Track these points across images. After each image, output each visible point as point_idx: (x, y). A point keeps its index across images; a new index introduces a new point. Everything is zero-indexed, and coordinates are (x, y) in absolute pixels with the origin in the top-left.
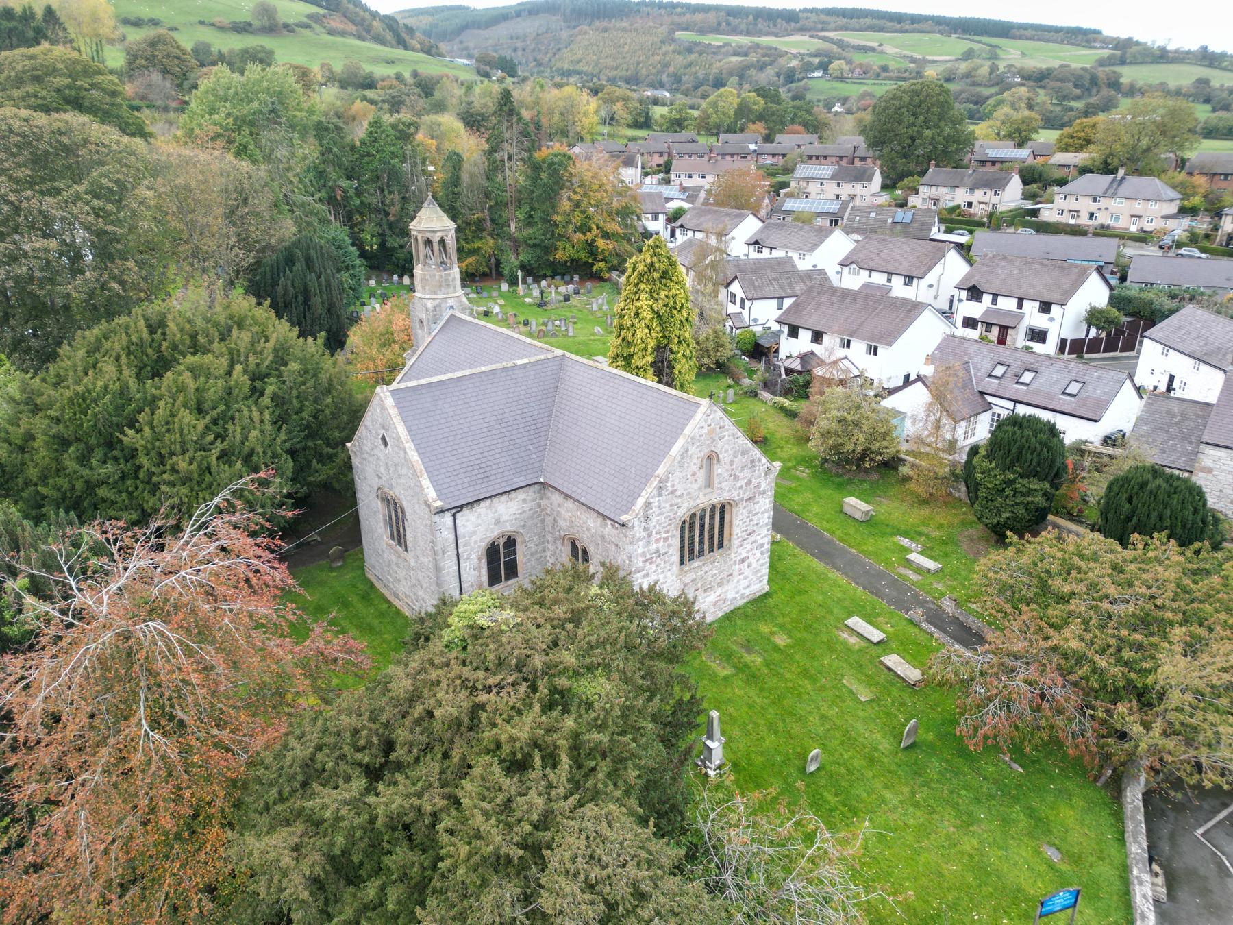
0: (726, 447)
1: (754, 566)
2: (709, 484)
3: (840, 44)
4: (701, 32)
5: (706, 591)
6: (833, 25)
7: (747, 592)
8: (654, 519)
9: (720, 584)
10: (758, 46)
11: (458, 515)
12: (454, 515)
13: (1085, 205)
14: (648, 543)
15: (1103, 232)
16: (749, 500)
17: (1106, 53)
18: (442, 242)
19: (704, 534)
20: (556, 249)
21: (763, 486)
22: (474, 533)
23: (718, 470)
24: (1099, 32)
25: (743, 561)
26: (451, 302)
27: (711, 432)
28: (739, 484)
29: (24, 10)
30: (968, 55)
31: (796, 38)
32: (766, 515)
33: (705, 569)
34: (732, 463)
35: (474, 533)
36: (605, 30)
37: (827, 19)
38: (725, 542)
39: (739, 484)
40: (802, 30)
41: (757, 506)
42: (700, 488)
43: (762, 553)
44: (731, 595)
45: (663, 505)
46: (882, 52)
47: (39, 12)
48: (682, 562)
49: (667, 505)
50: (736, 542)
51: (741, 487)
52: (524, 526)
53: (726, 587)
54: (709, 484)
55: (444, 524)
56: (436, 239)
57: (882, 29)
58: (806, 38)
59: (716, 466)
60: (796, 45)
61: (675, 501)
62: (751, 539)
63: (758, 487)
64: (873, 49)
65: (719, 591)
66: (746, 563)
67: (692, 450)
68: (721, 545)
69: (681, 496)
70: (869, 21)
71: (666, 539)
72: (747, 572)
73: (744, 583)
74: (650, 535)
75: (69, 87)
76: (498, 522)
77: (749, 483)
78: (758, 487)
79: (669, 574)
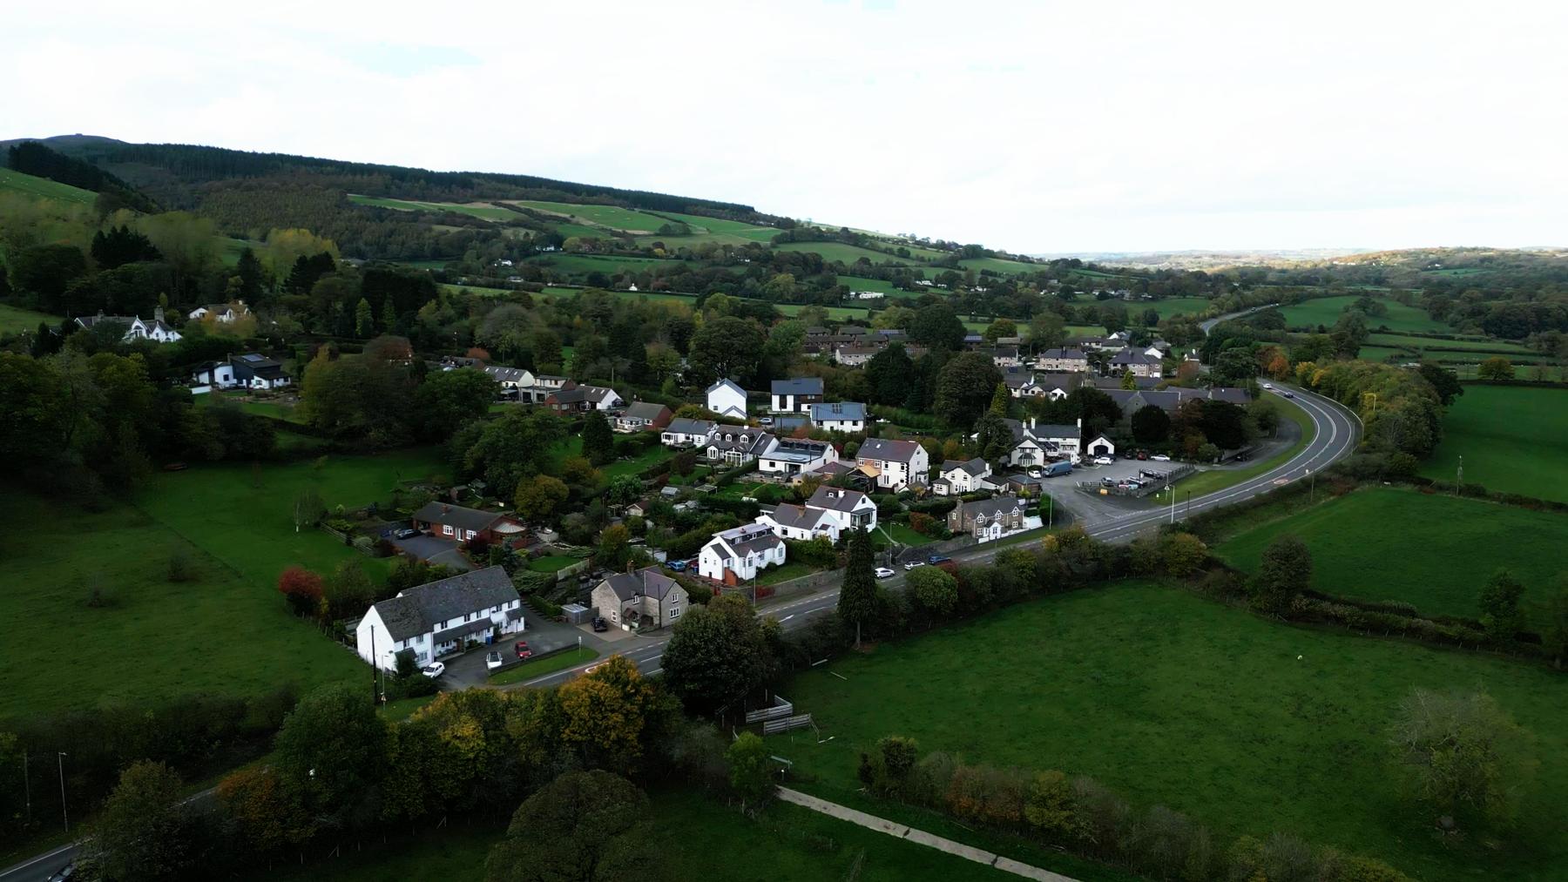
3: (528, 212)
4: (373, 195)
6: (512, 194)
10: (453, 214)
13: (1053, 362)
15: (1064, 372)
17: (779, 232)
24: (752, 209)
30: (666, 232)
31: (479, 205)
36: (249, 188)
37: (507, 187)
40: (482, 197)
46: (577, 224)
57: (563, 200)
58: (489, 206)
60: (482, 209)
64: (566, 220)
70: (549, 192)
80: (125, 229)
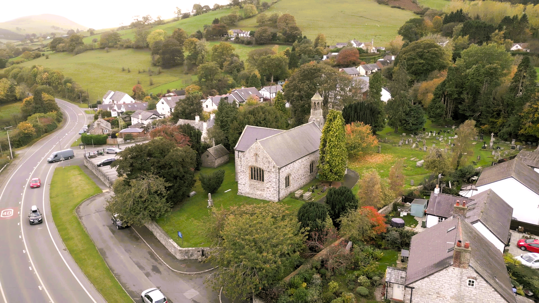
2: (256, 161)
7: (270, 198)
8: (242, 163)
9: (261, 190)
18: (315, 103)
19: (257, 174)
20: (521, 129)
21: (273, 170)
23: (259, 159)
25: (268, 188)
26: (314, 119)
27: (256, 148)
29: (514, 17)
33: (256, 183)
44: (265, 196)
47: (520, 17)
48: (252, 178)
54: (256, 161)
56: (313, 102)
62: (270, 183)
65: (261, 192)
67: (251, 150)
68: (263, 181)
73: (268, 195)
75: (421, 52)
77: (268, 167)
80: (461, 10)
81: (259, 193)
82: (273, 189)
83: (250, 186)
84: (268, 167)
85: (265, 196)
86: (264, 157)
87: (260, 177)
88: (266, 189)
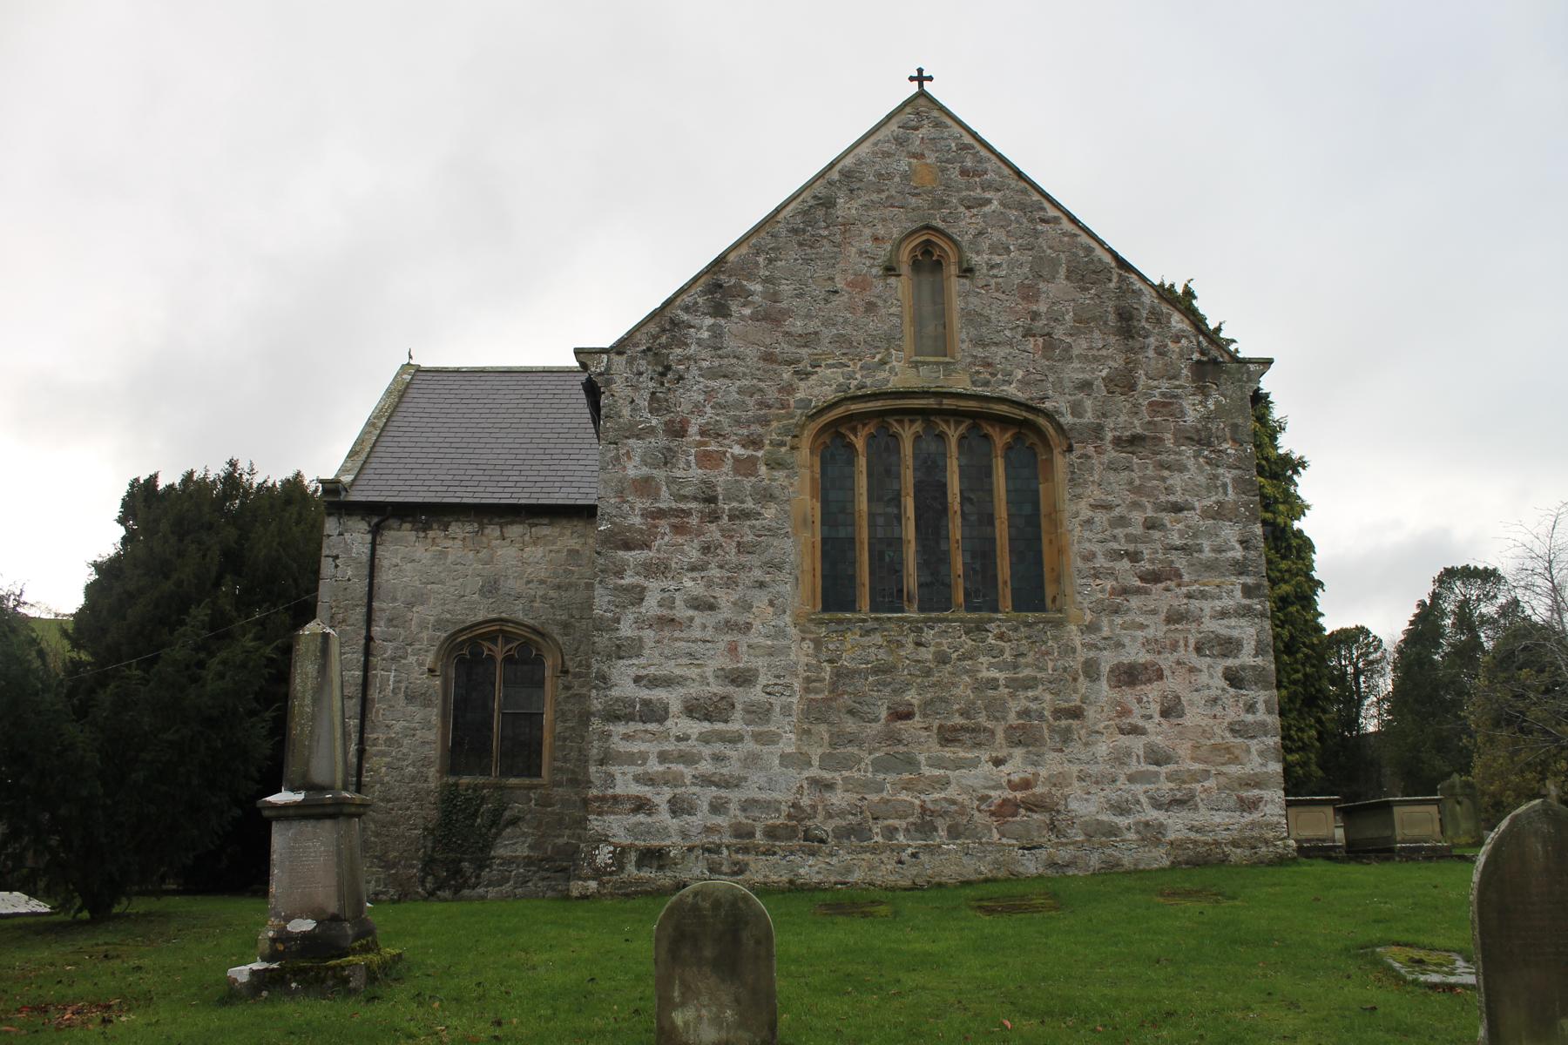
0: (997, 235)
1: (1194, 717)
5: (948, 737)
7: (1177, 824)
9: (1023, 737)
11: (389, 535)
12: (376, 531)
14: (667, 459)
16: (1132, 442)
22: (418, 599)
25: (1129, 676)
28: (1074, 372)
32: (1230, 533)
34: (1029, 293)
35: (418, 599)
38: (1049, 590)
39: (1074, 372)
41: (1176, 480)
42: (890, 340)
43: (1234, 679)
44: (1085, 806)
45: (731, 344)
48: (836, 594)
49: (751, 353)
50: (1083, 594)
51: (1086, 386)
52: (566, 626)
53: (1052, 764)
55: (348, 550)
59: (956, 285)
61: (784, 348)
62: (1163, 598)
63: (1167, 406)
66: (1153, 693)
68: (1033, 593)
69: (808, 339)
71: (745, 467)
72: (1158, 733)
74: (677, 430)
76: (490, 588)
77: (1123, 383)
78: (1167, 406)
79: (760, 600)
81: (979, 776)
82: (1212, 674)
83: (815, 712)
84: (1123, 383)
85: (1085, 806)
86: (1042, 269)
87: (982, 555)
88: (1104, 689)
